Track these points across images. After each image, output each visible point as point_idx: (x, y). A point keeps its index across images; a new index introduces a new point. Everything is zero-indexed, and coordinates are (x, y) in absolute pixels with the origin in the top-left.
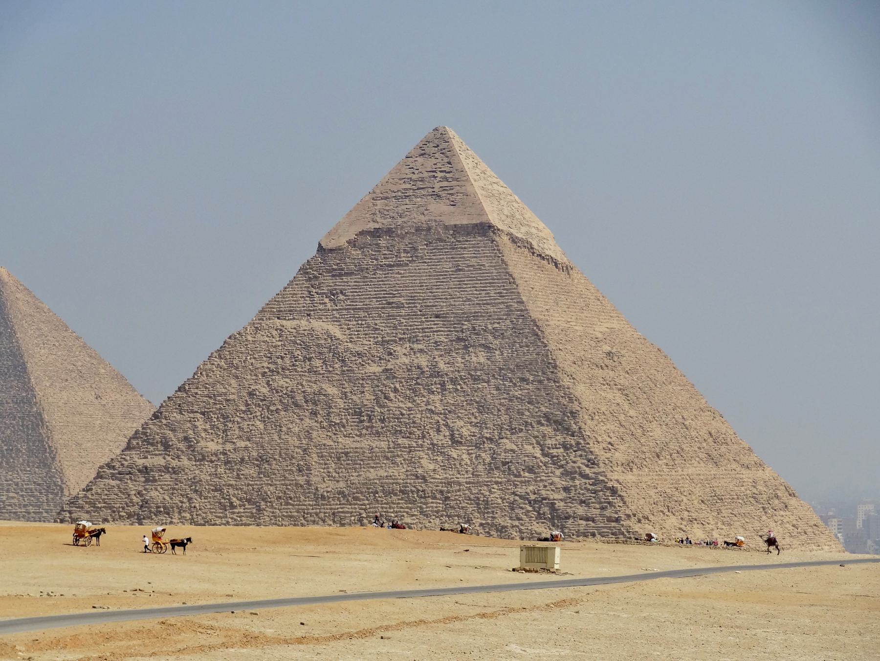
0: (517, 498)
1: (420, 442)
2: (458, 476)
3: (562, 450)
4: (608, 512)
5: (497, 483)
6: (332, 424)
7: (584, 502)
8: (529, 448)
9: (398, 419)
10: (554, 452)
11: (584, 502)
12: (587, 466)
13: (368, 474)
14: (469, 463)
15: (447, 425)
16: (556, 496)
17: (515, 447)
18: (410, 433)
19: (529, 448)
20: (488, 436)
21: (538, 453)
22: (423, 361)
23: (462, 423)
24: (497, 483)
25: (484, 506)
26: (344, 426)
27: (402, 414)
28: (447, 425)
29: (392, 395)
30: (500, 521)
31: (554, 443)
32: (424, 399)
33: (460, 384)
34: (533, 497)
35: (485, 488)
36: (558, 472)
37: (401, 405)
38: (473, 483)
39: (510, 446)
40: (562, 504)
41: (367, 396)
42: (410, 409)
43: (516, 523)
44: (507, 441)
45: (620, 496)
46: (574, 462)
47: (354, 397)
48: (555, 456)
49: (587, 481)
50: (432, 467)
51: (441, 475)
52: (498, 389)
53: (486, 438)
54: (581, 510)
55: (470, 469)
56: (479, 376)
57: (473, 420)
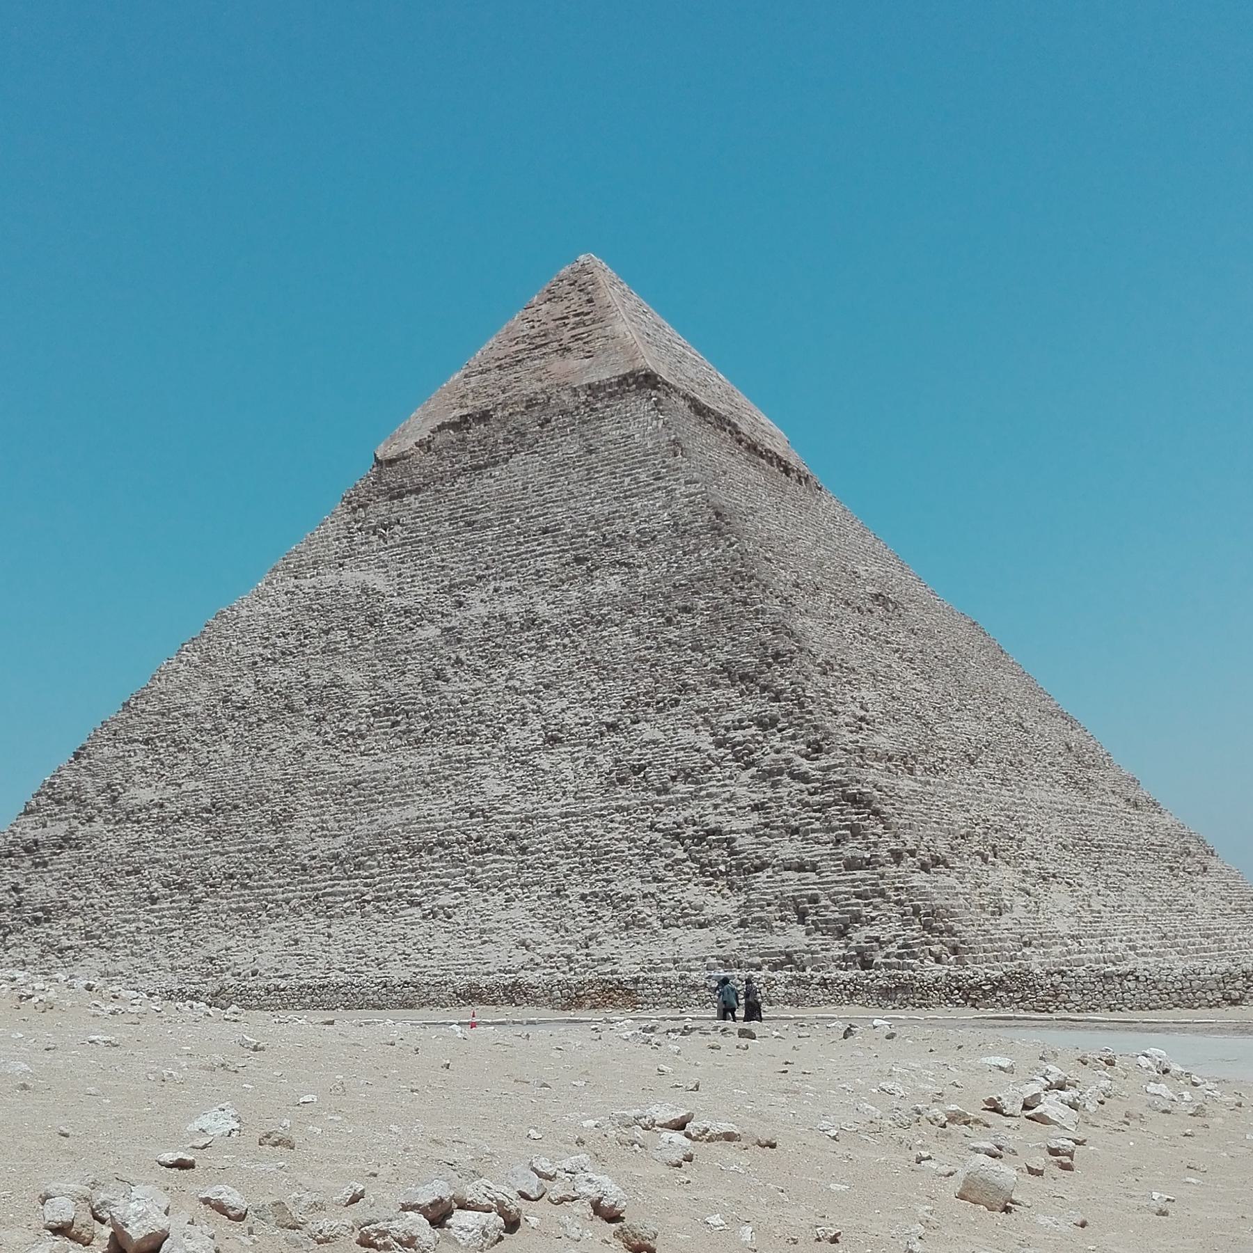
0: (658, 836)
1: (487, 748)
2: (549, 803)
3: (754, 730)
4: (851, 849)
5: (619, 809)
6: (342, 735)
7: (796, 831)
8: (687, 736)
9: (453, 711)
10: (738, 735)
11: (796, 831)
12: (806, 757)
13: (388, 817)
14: (571, 776)
15: (538, 711)
16: (737, 824)
17: (660, 736)
18: (474, 734)
19: (687, 736)
20: (610, 720)
21: (705, 740)
22: (511, 606)
23: (565, 703)
24: (619, 809)
25: (596, 858)
26: (362, 737)
27: (463, 702)
28: (538, 711)
29: (449, 671)
30: (621, 888)
31: (737, 717)
32: (504, 671)
33: (570, 636)
34: (690, 831)
35: (596, 822)
36: (745, 776)
37: (463, 686)
38: (574, 814)
39: (648, 732)
40: (750, 838)
41: (409, 678)
42: (476, 692)
43: (652, 888)
44: (647, 726)
45: (876, 813)
46: (778, 752)
47: (388, 685)
48: (739, 744)
49: (803, 786)
50: (500, 791)
51: (517, 806)
52: (637, 632)
53: (607, 725)
54: (789, 849)
55: (570, 788)
56: (603, 616)
57: (588, 695)
